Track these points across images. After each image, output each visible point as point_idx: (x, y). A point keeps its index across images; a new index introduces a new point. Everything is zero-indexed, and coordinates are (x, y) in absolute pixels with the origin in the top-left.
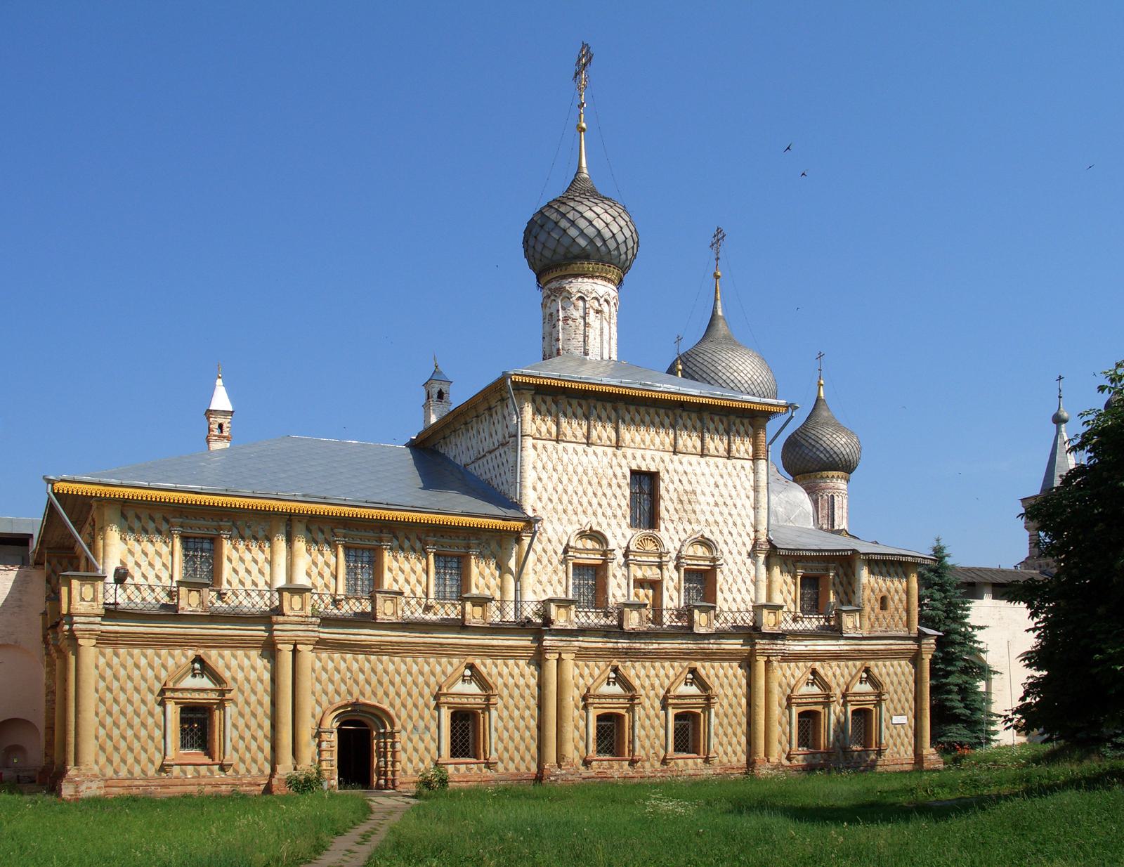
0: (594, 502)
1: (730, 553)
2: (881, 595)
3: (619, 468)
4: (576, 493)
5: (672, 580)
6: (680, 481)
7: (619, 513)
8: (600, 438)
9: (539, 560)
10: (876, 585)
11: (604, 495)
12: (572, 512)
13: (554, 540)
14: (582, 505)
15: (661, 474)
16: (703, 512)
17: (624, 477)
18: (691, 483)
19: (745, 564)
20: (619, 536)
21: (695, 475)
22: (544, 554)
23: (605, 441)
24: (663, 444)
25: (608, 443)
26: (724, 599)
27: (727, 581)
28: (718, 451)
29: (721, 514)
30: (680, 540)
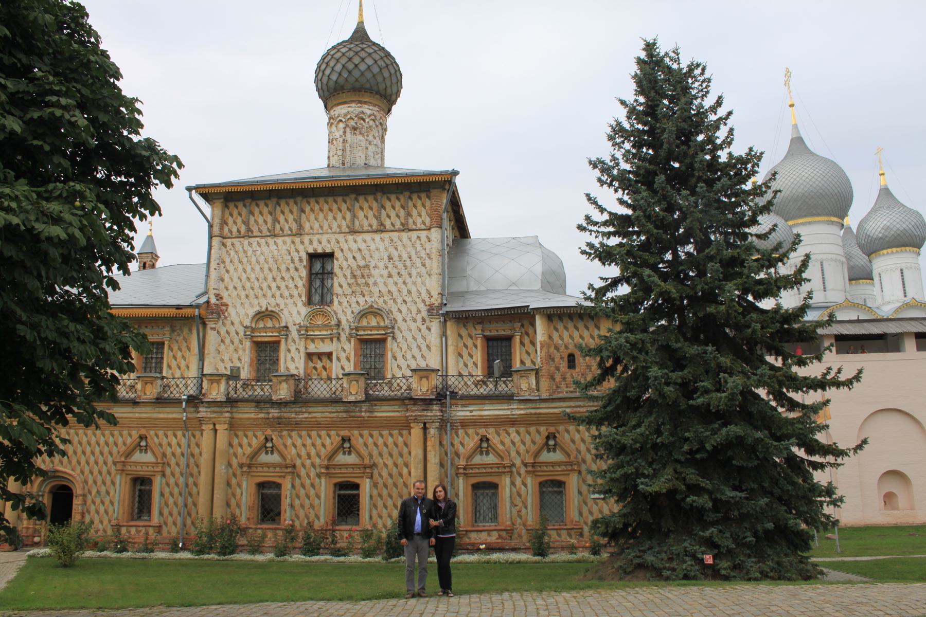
0: (274, 285)
1: (405, 320)
2: (569, 351)
3: (296, 254)
4: (258, 280)
5: (344, 350)
6: (354, 258)
7: (295, 293)
8: (282, 229)
9: (223, 341)
10: (560, 342)
11: (283, 278)
12: (254, 296)
13: (236, 322)
14: (262, 289)
15: (336, 254)
16: (375, 284)
17: (301, 260)
18: (364, 258)
19: (420, 331)
20: (295, 314)
21: (369, 250)
22: (227, 335)
23: (287, 231)
24: (339, 226)
25: (290, 232)
26: (398, 366)
27: (401, 348)
28: (393, 225)
29: (396, 284)
30: (352, 312)
